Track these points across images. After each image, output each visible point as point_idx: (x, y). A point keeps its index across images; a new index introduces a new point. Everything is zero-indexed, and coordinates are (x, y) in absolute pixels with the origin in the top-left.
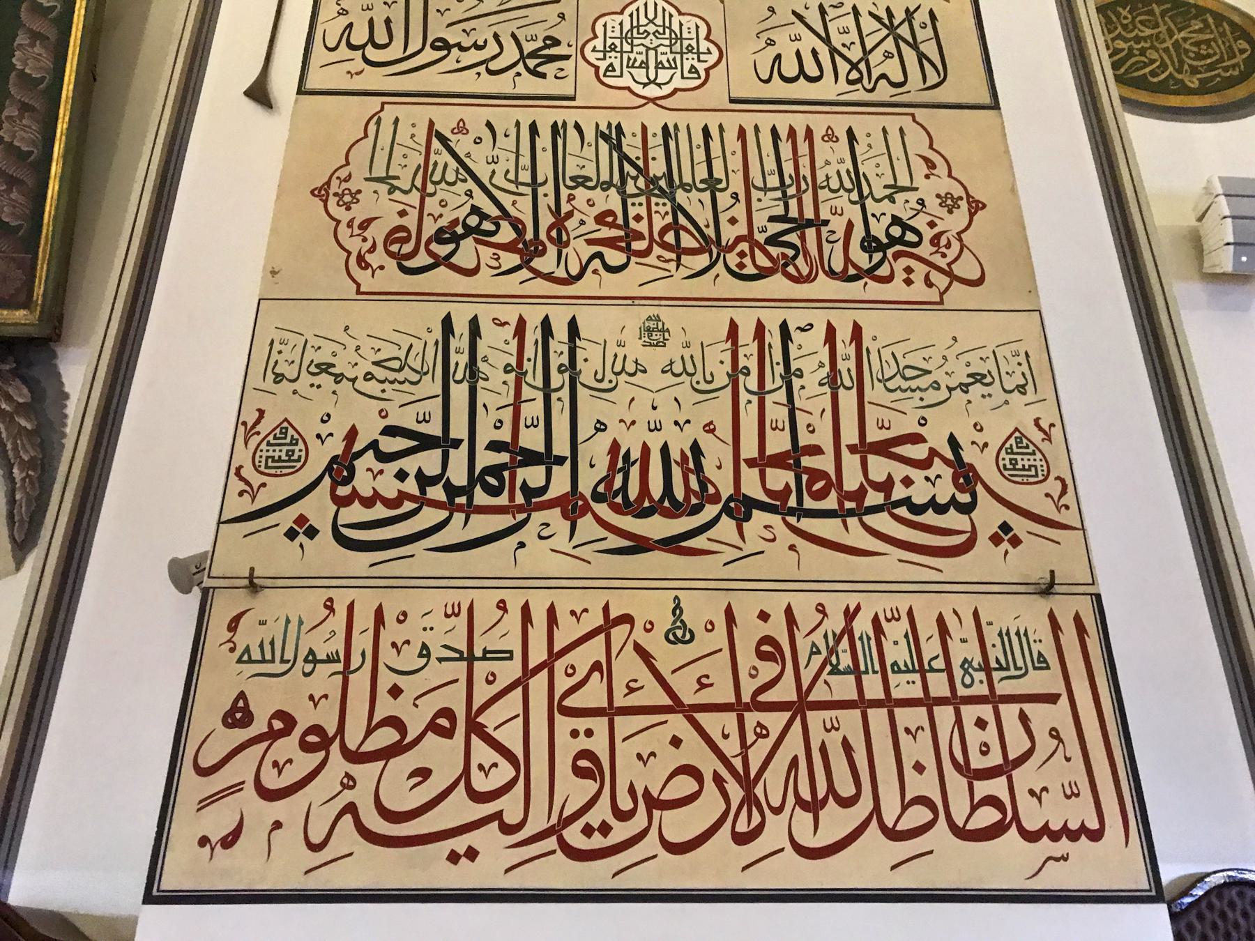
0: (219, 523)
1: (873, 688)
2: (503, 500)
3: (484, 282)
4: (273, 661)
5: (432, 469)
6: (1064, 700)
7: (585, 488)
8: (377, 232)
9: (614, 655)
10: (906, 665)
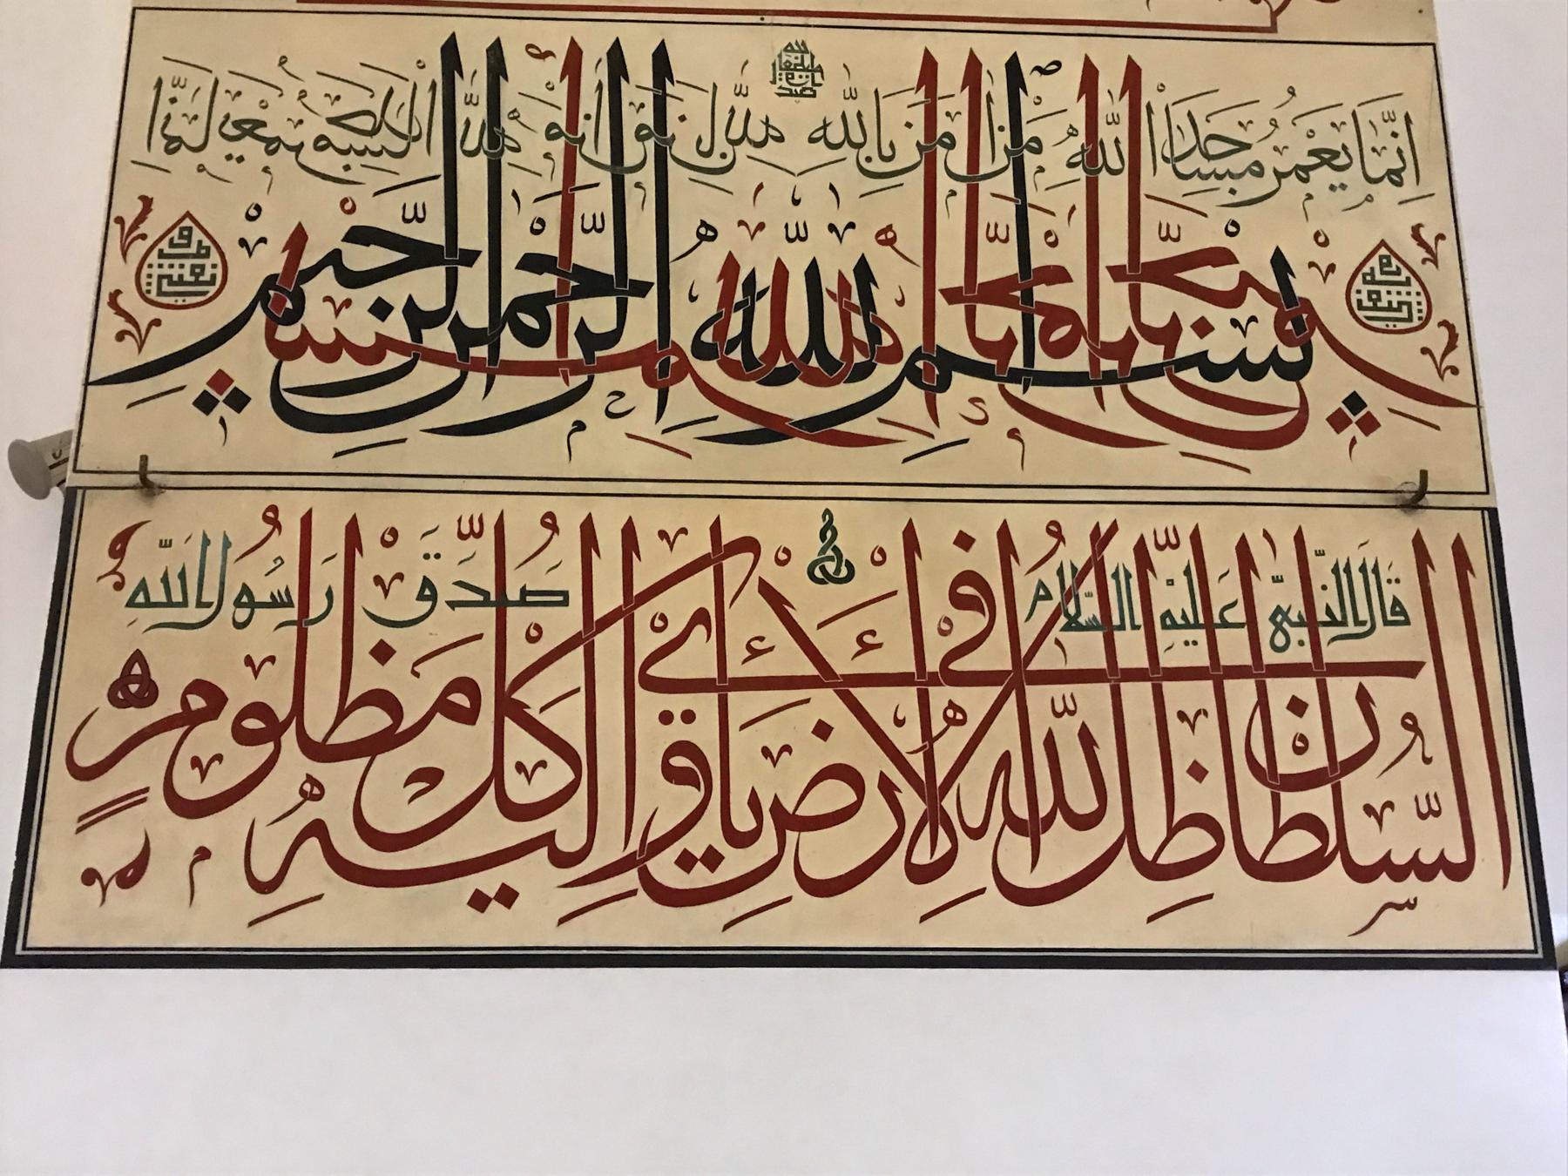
0: (87, 383)
1: (1131, 650)
2: (548, 352)
4: (184, 604)
5: (431, 299)
6: (1429, 671)
7: (682, 335)
9: (727, 600)
10: (1184, 616)
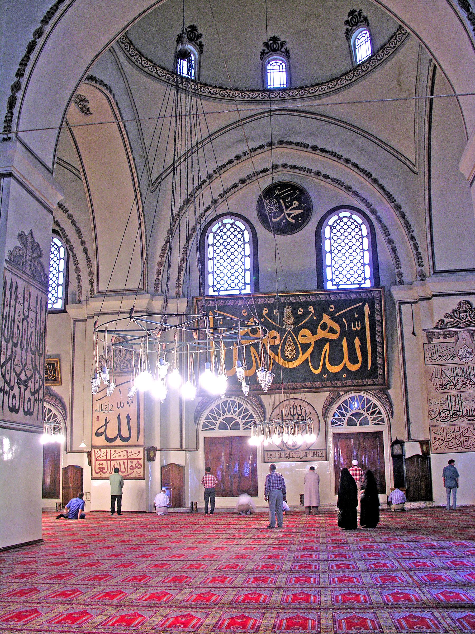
3: (450, 390)
8: (438, 385)
